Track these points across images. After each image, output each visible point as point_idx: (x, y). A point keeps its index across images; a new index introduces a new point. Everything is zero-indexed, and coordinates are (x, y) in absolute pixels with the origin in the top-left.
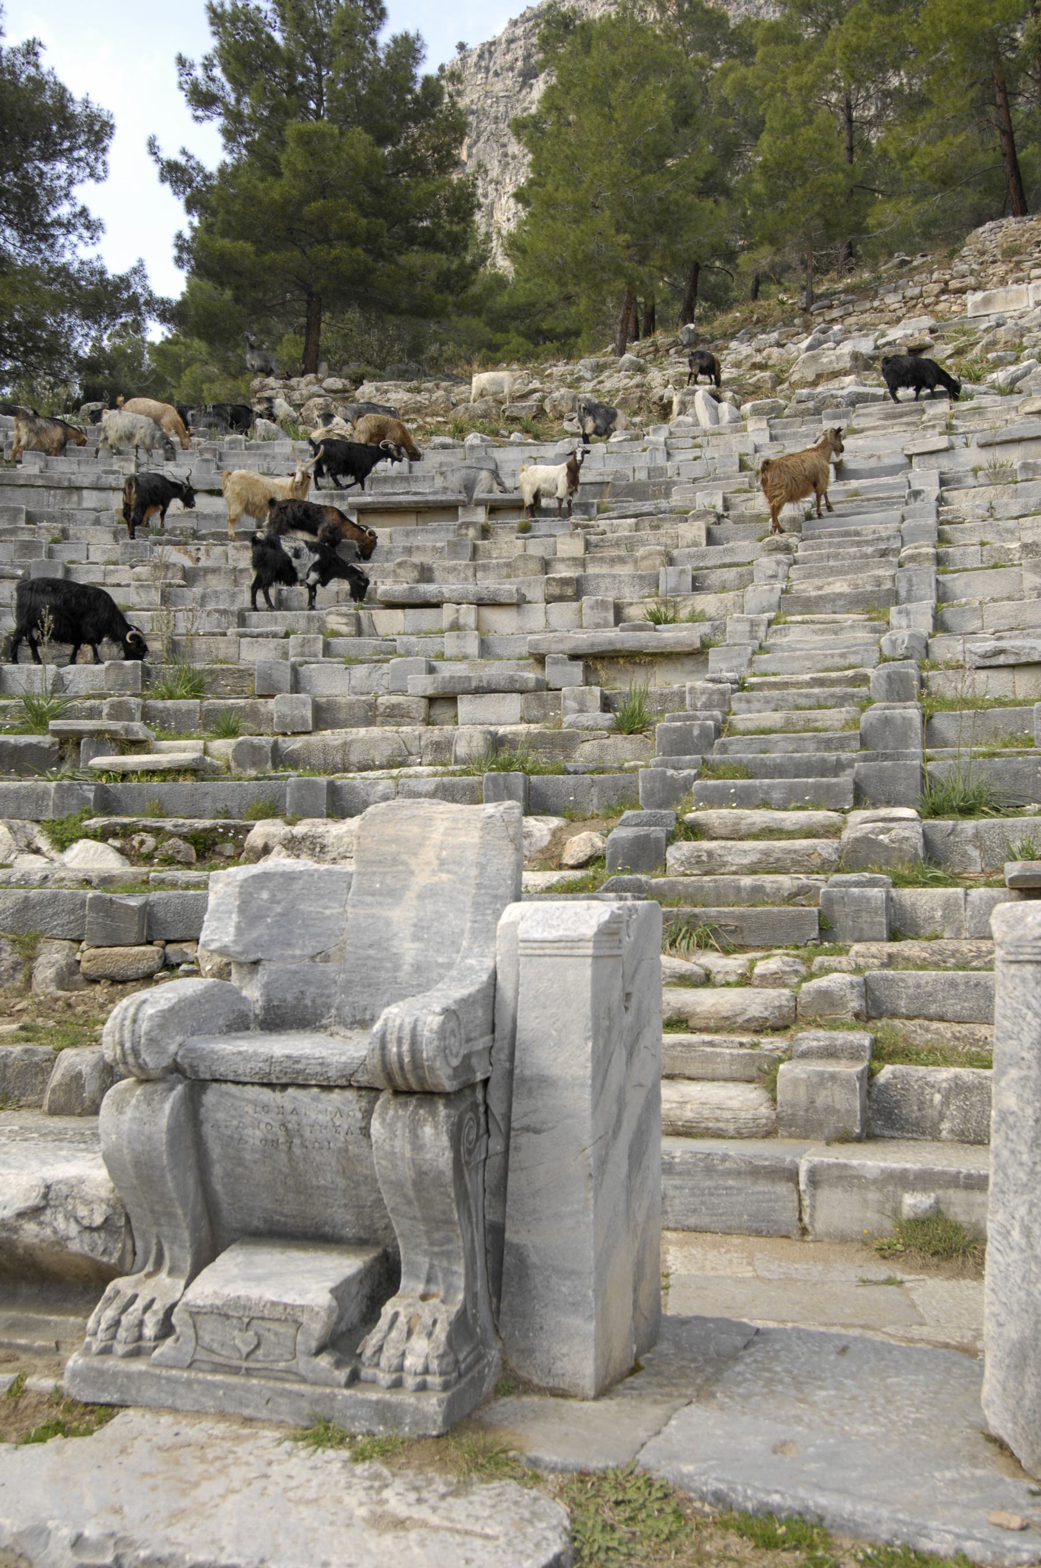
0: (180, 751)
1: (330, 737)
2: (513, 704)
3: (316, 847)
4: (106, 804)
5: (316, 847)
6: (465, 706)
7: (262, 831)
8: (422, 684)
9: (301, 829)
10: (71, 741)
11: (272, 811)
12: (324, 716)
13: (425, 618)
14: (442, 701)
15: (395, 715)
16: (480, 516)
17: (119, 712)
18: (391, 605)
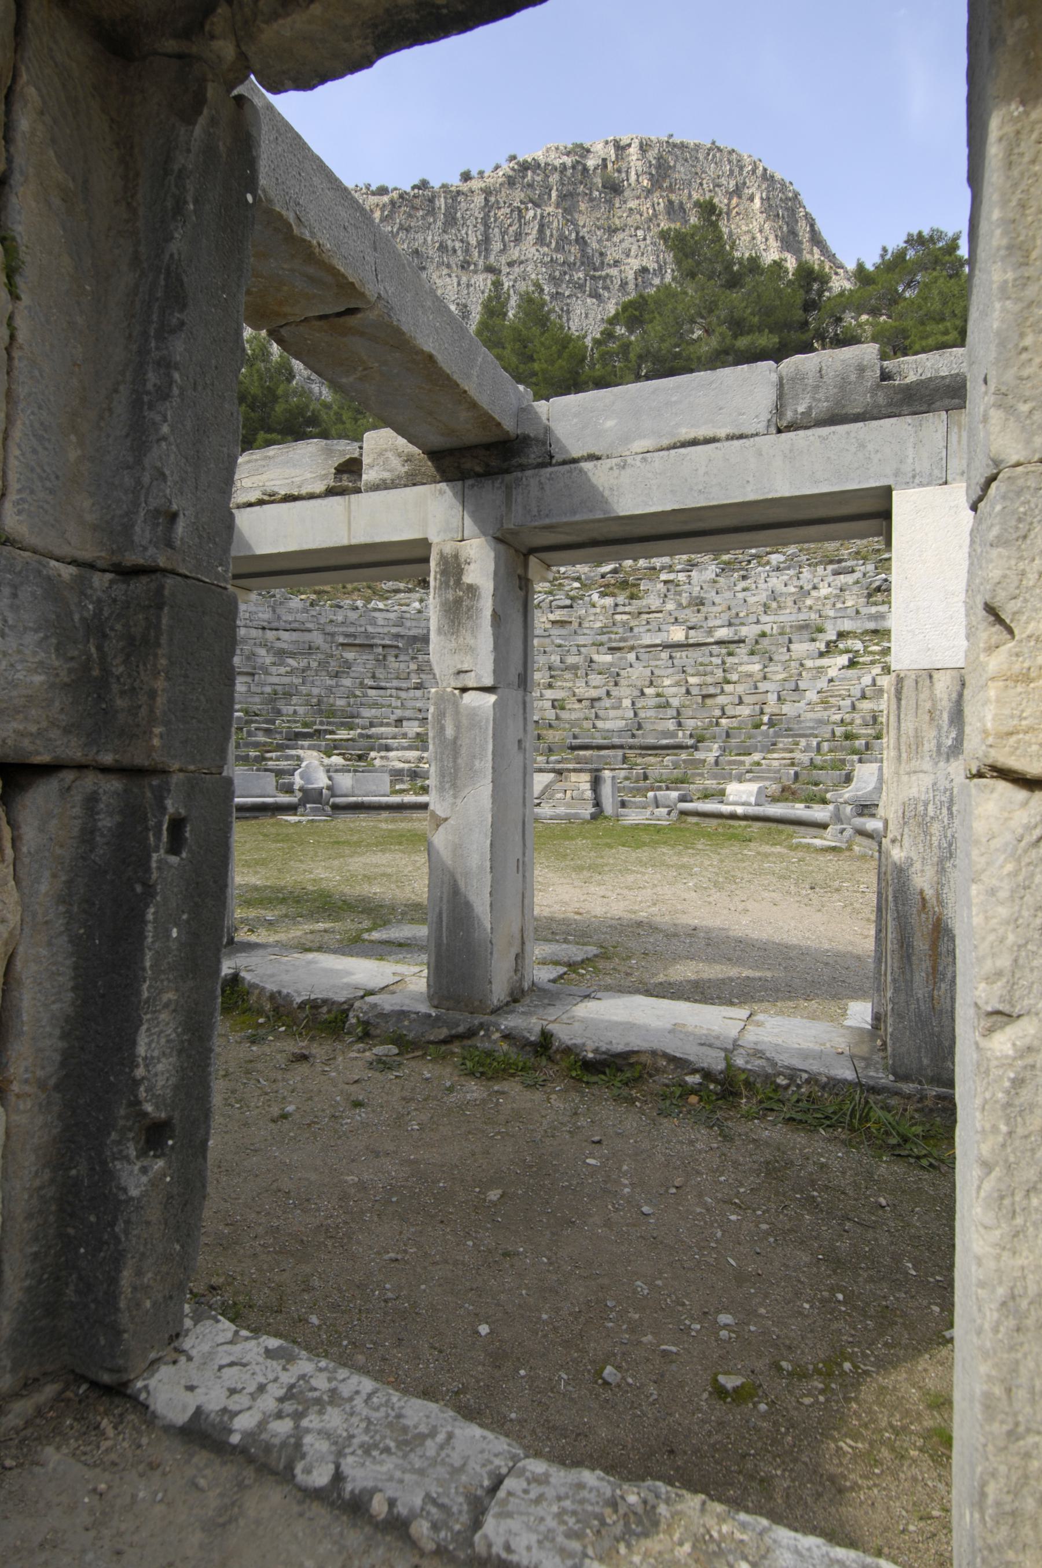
0: (343, 734)
1: (374, 730)
2: (416, 723)
3: (386, 758)
4: (336, 748)
5: (386, 758)
6: (405, 723)
7: (373, 754)
8: (394, 717)
9: (383, 754)
10: (318, 731)
11: (372, 749)
12: (372, 725)
13: (381, 692)
14: (399, 722)
15: (388, 725)
16: (380, 650)
17: (322, 723)
18: (372, 688)
